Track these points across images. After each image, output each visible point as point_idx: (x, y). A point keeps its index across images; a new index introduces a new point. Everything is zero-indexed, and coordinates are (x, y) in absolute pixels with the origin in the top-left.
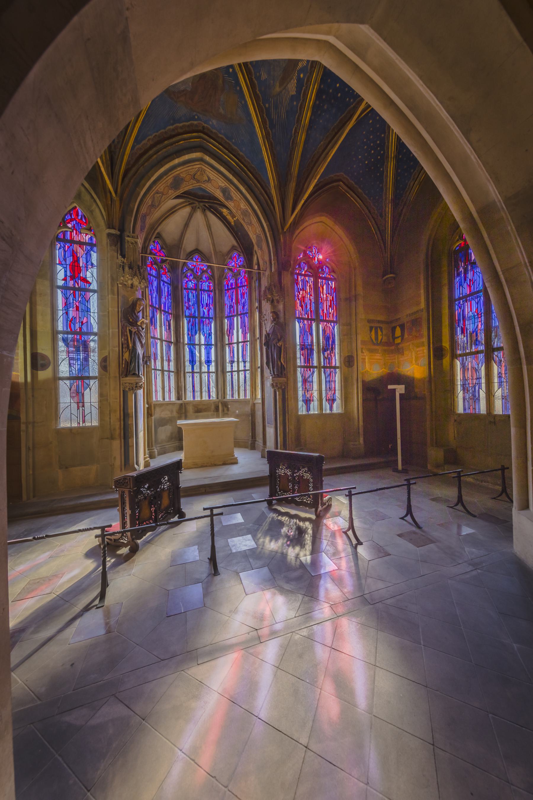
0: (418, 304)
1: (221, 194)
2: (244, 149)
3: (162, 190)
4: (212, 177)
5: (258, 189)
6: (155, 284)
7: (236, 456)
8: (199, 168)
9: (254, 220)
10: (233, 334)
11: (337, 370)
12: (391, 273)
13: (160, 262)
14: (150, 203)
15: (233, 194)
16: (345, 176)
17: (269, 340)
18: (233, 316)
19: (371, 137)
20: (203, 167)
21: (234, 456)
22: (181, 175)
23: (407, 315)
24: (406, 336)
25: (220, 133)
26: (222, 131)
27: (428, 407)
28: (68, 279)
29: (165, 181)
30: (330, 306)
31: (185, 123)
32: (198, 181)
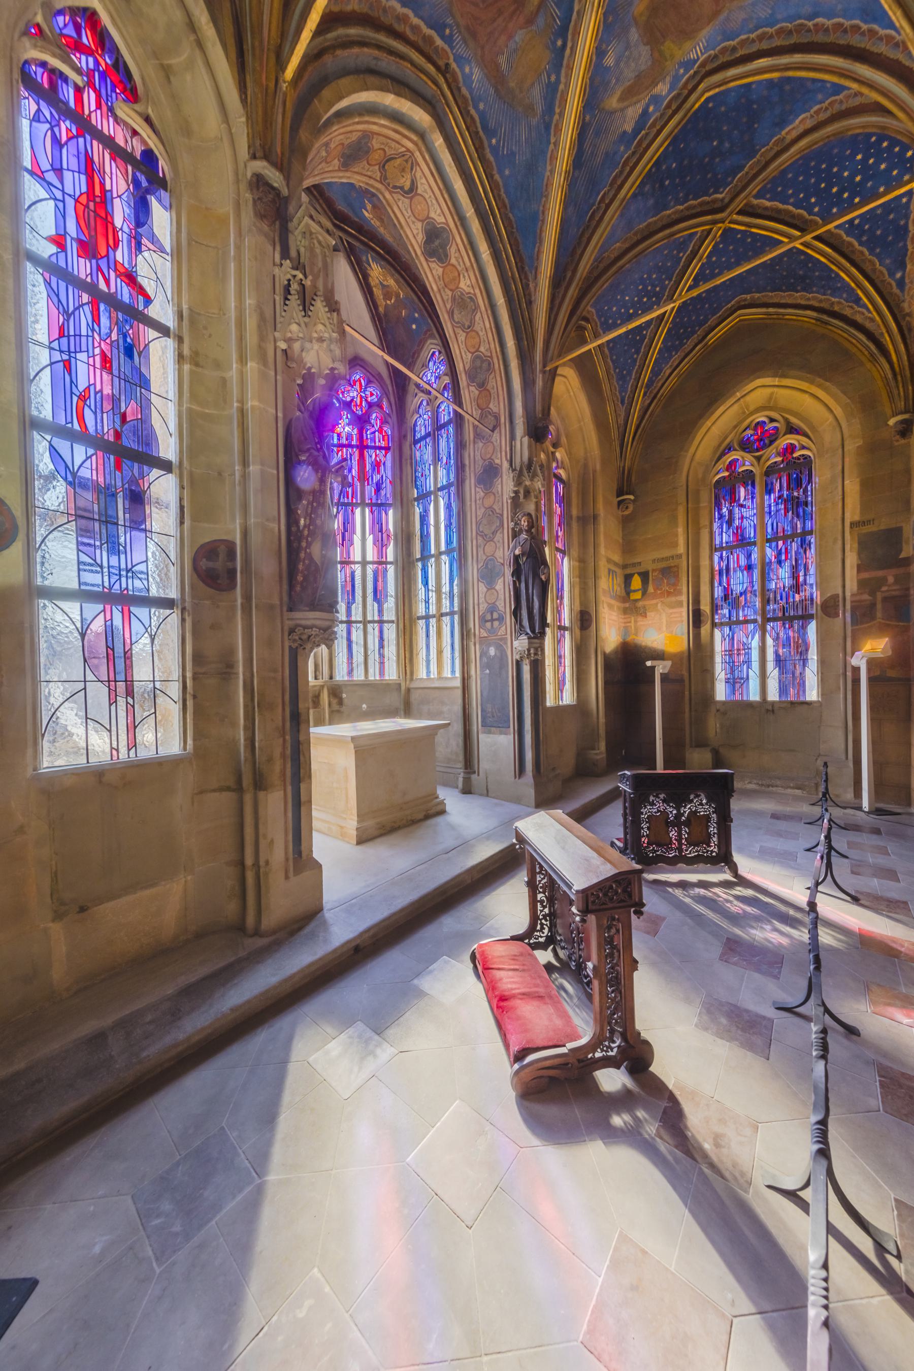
0: (675, 545)
2: (507, 172)
4: (422, 187)
7: (441, 797)
8: (408, 150)
9: (483, 323)
10: (352, 544)
11: (566, 632)
12: (627, 494)
16: (595, 317)
18: (353, 505)
19: (654, 276)
20: (417, 154)
21: (437, 797)
23: (654, 561)
24: (651, 589)
25: (476, 107)
26: (481, 106)
27: (687, 693)
30: (559, 525)
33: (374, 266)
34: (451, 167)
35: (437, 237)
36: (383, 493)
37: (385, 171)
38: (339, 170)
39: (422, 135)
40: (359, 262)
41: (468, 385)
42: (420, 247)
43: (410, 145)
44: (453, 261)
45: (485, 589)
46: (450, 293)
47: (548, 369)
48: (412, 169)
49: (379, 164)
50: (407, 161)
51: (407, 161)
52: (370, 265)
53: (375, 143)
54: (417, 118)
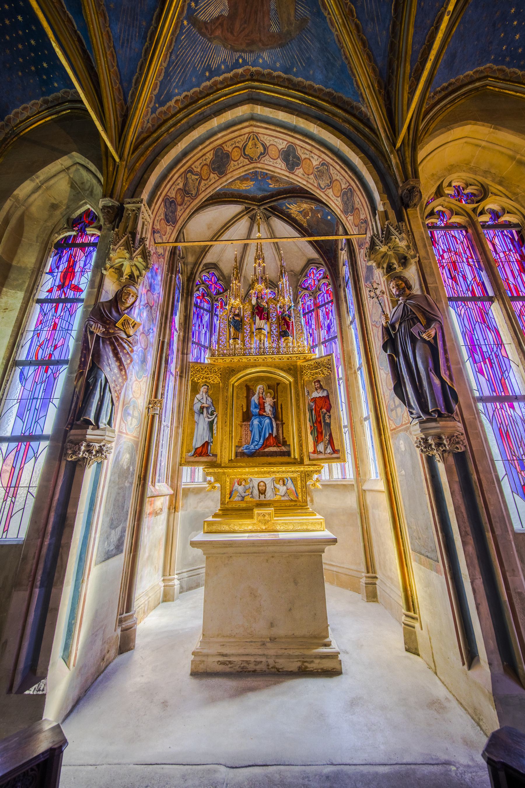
1: (284, 166)
3: (199, 170)
4: (268, 141)
5: (339, 118)
6: (206, 318)
8: (249, 133)
13: (215, 295)
14: (181, 186)
15: (299, 152)
17: (395, 335)
20: (256, 129)
22: (226, 148)
28: (55, 289)
29: (201, 154)
31: (226, 75)
32: (251, 160)
33: (291, 207)
34: (271, 113)
35: (289, 155)
36: (332, 330)
37: (248, 155)
38: (220, 178)
39: (252, 118)
40: (282, 212)
41: (347, 218)
42: (286, 171)
43: (247, 130)
44: (303, 156)
45: (385, 376)
46: (312, 176)
47: (398, 145)
48: (258, 139)
49: (241, 155)
50: (253, 139)
51: (253, 139)
52: (289, 208)
53: (228, 148)
54: (241, 114)
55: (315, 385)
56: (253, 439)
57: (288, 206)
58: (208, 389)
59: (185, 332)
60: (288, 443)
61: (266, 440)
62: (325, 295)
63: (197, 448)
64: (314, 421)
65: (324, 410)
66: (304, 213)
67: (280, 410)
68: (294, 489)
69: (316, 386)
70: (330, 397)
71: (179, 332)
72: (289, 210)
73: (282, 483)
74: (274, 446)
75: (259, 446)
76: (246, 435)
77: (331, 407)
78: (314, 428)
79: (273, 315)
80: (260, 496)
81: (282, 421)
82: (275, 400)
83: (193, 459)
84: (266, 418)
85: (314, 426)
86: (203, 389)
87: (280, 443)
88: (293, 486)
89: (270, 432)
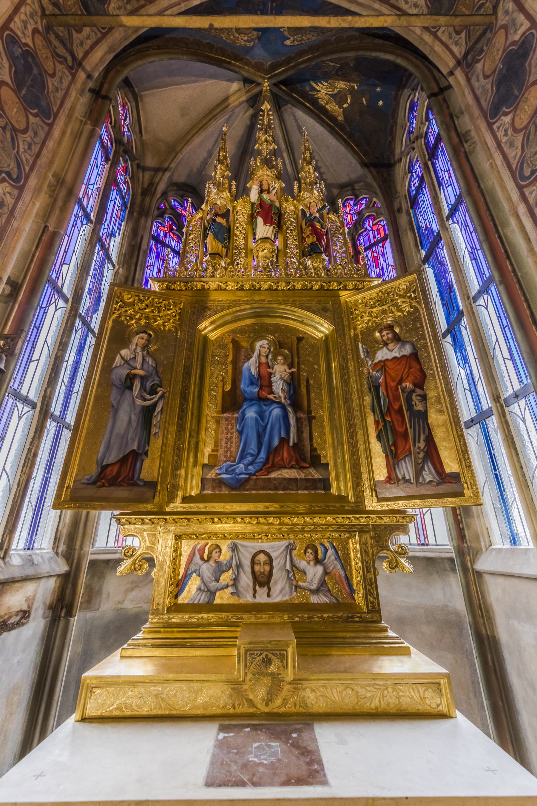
52: (316, 90)
55: (382, 336)
56: (243, 450)
57: (314, 85)
58: (149, 341)
59: (128, 269)
60: (323, 461)
61: (272, 452)
62: (371, 233)
63: (108, 466)
64: (384, 409)
65: (408, 385)
66: (339, 98)
67: (304, 390)
68: (342, 573)
69: (385, 338)
70: (422, 354)
71: (117, 267)
72: (315, 93)
73: (312, 557)
74: (292, 467)
75: (258, 466)
76: (228, 440)
77: (424, 376)
78: (385, 426)
79: (290, 220)
80: (255, 591)
81: (309, 412)
82: (294, 370)
83: (91, 491)
84: (275, 405)
85: (385, 421)
86: (138, 340)
87: (304, 460)
88: (339, 566)
89: (283, 435)
